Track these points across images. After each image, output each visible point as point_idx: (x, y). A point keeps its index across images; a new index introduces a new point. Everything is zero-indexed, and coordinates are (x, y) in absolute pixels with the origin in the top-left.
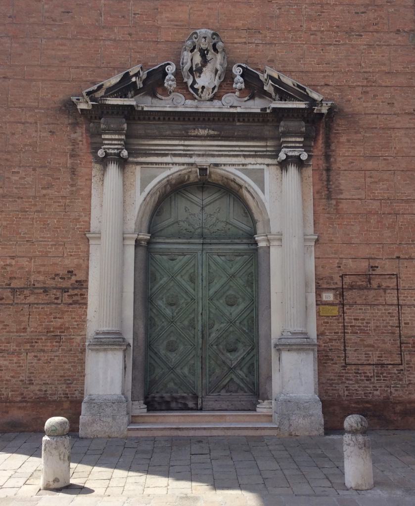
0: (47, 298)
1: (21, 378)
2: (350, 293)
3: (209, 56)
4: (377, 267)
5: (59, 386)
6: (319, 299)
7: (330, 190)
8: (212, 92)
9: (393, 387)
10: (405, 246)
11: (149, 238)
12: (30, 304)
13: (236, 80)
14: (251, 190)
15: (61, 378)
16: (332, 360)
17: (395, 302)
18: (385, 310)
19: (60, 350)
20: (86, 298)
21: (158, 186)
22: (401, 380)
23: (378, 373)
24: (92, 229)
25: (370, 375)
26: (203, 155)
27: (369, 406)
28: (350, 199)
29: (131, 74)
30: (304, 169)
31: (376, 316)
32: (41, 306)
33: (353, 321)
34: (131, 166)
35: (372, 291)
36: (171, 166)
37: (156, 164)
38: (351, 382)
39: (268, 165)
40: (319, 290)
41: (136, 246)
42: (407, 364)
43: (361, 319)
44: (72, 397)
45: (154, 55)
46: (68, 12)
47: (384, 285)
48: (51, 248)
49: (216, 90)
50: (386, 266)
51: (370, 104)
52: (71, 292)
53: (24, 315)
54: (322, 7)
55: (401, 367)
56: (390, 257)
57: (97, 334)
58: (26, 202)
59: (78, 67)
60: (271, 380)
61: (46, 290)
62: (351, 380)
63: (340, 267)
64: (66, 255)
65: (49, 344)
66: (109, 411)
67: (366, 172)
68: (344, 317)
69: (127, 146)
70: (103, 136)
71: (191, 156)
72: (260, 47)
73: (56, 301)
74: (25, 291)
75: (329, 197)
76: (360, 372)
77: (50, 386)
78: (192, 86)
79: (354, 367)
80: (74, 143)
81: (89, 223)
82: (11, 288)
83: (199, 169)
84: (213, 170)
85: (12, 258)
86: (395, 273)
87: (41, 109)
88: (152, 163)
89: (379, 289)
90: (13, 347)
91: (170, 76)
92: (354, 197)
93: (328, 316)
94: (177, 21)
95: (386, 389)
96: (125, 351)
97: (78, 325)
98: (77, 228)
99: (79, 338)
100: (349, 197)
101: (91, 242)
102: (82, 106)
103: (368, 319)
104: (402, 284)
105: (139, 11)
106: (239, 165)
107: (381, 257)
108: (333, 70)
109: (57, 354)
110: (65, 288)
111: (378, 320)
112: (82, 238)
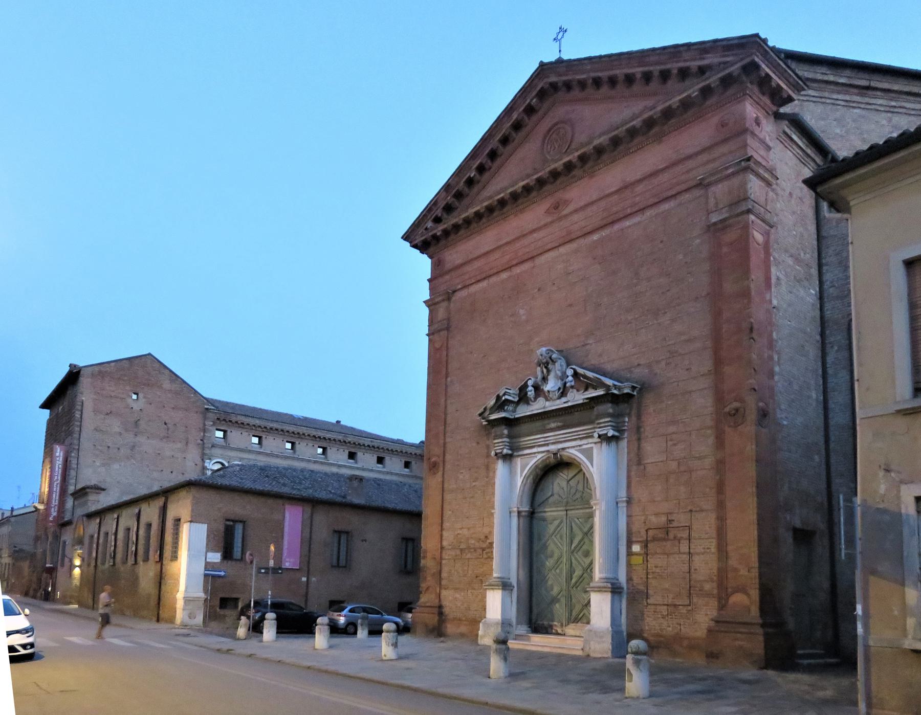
2: (652, 544)
22: (689, 619)
25: (665, 614)
33: (654, 568)
36: (537, 454)
39: (595, 443)
55: (690, 608)
71: (547, 445)
79: (653, 607)
84: (561, 453)
88: (527, 454)
91: (530, 388)
104: (693, 534)
106: (577, 446)
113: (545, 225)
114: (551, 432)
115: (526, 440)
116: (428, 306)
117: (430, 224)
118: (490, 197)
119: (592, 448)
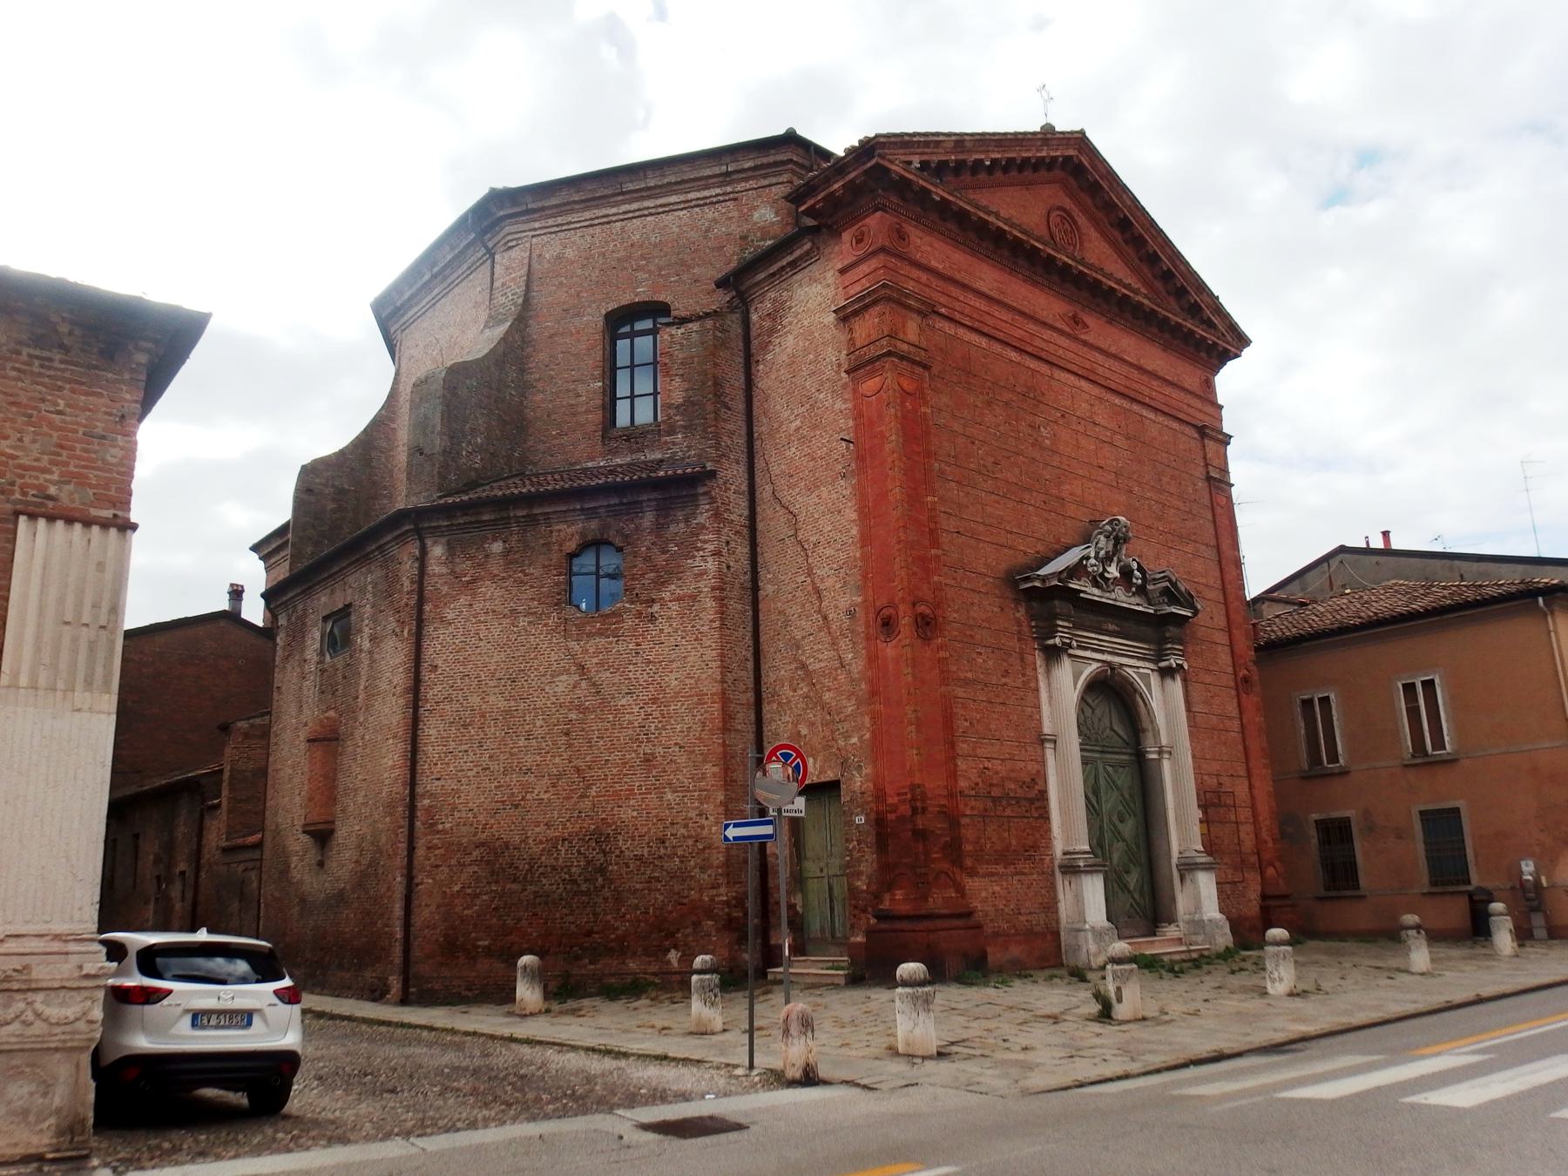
1: (1012, 907)
12: (1008, 817)
59: (1011, 533)
80: (1018, 622)
81: (1040, 721)
87: (990, 577)
99: (1048, 858)
118: (977, 207)
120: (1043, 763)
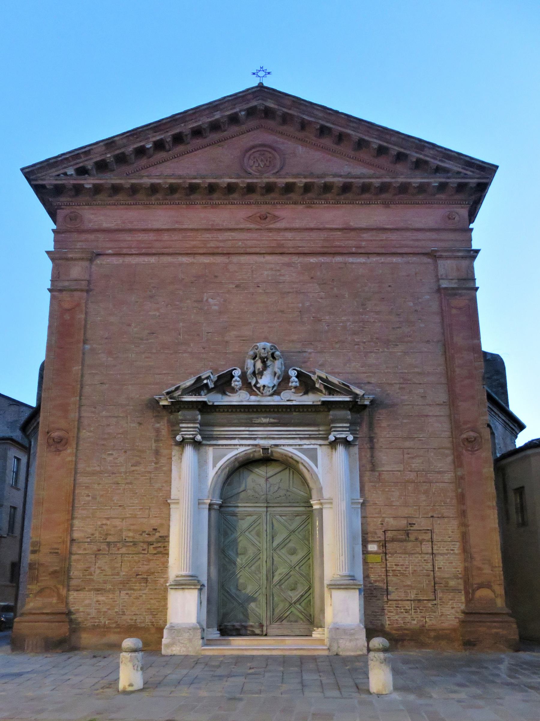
0: (136, 549)
1: (116, 610)
3: (269, 363)
4: (415, 524)
5: (146, 616)
6: (365, 549)
7: (374, 464)
8: (272, 389)
9: (428, 618)
10: (437, 507)
11: (220, 502)
12: (122, 554)
13: (292, 379)
14: (306, 465)
15: (148, 610)
16: (376, 597)
17: (430, 551)
18: (421, 557)
19: (147, 589)
20: (168, 550)
21: (227, 463)
22: (435, 612)
23: (415, 607)
24: (172, 497)
25: (408, 608)
26: (265, 438)
27: (406, 632)
28: (390, 471)
29: (203, 377)
30: (351, 448)
31: (414, 563)
32: (131, 556)
33: (394, 566)
34: (204, 447)
35: (410, 543)
36: (238, 447)
37: (226, 445)
38: (392, 614)
39: (320, 445)
40: (365, 543)
41: (210, 509)
42: (440, 599)
43: (401, 565)
44: (157, 625)
45: (224, 363)
46: (153, 333)
47: (420, 538)
48: (139, 512)
49: (275, 389)
50: (423, 523)
51: (406, 397)
52: (155, 545)
53: (117, 563)
54: (364, 324)
55: (435, 602)
56: (426, 516)
57: (177, 577)
58: (119, 476)
60: (324, 613)
61: (135, 544)
62: (392, 612)
63: (382, 524)
64: (151, 516)
65: (138, 584)
66: (186, 635)
67: (405, 450)
68: (386, 563)
69: (201, 432)
70: (181, 425)
71: (255, 439)
72: (313, 355)
73: (143, 552)
74: (118, 544)
75: (373, 470)
76: (400, 606)
77: (140, 616)
78: (255, 385)
79: (394, 602)
80: (158, 431)
82: (107, 542)
83: (262, 449)
85: (108, 519)
86: (429, 529)
88: (223, 445)
89: (417, 541)
90: (109, 586)
91: (236, 378)
92: (394, 469)
93: (373, 563)
94: (243, 337)
95: (422, 619)
96: (200, 590)
97: (161, 570)
98: (160, 496)
100: (390, 470)
101: (172, 506)
102: (163, 403)
103: (408, 565)
104: (435, 537)
105: (211, 331)
106: (296, 445)
107: (417, 516)
108: (374, 371)
109: (145, 592)
110: (151, 542)
111: (415, 566)
112: (164, 503)
113: (249, 230)
114: (264, 426)
115: (218, 430)
116: (53, 259)
117: (71, 171)
119: (316, 449)
120: (168, 518)
